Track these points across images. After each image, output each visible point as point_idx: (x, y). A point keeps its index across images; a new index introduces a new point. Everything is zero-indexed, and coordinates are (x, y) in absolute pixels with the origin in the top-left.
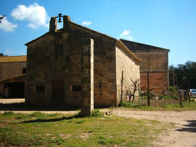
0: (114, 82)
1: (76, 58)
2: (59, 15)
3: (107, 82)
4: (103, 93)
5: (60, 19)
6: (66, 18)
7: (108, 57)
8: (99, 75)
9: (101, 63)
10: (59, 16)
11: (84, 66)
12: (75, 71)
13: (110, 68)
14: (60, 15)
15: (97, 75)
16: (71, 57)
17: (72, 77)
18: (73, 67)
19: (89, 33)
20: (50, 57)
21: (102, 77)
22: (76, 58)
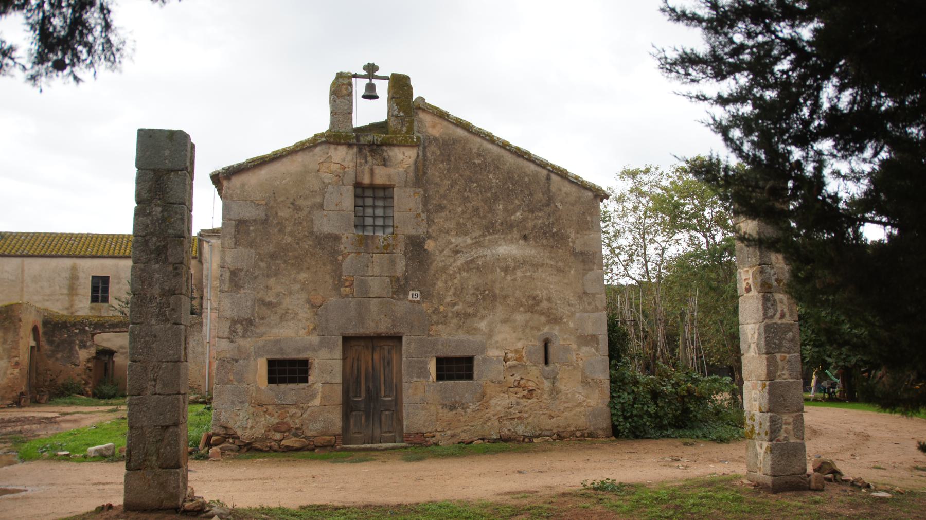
0: (598, 344)
1: (451, 246)
2: (365, 68)
3: (574, 346)
4: (561, 385)
5: (371, 87)
6: (400, 85)
7: (574, 254)
8: (543, 319)
9: (550, 275)
10: (365, 73)
11: (773, 278)
12: (448, 299)
13: (585, 293)
14: (371, 69)
15: (536, 316)
16: (430, 245)
17: (437, 323)
18: (440, 284)
19: (499, 157)
20: (336, 238)
21: (557, 327)
22: (451, 246)
